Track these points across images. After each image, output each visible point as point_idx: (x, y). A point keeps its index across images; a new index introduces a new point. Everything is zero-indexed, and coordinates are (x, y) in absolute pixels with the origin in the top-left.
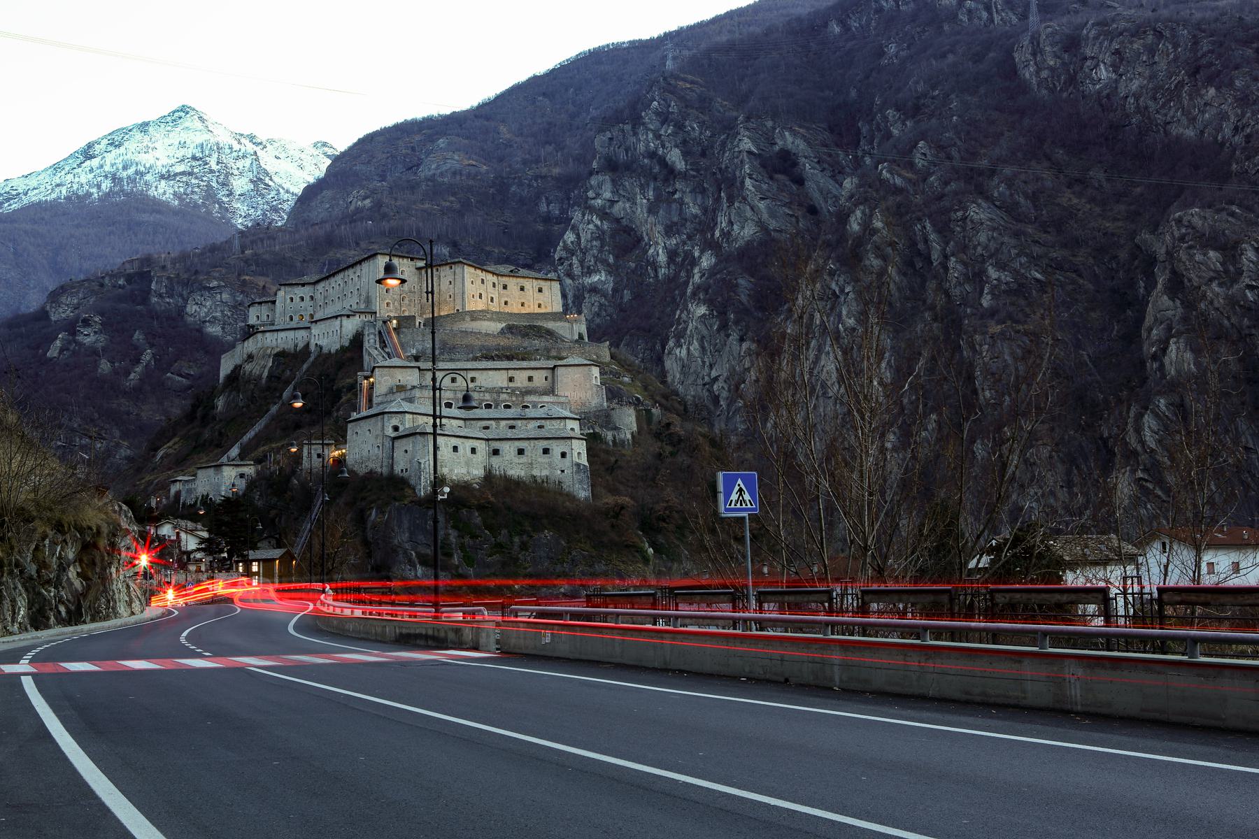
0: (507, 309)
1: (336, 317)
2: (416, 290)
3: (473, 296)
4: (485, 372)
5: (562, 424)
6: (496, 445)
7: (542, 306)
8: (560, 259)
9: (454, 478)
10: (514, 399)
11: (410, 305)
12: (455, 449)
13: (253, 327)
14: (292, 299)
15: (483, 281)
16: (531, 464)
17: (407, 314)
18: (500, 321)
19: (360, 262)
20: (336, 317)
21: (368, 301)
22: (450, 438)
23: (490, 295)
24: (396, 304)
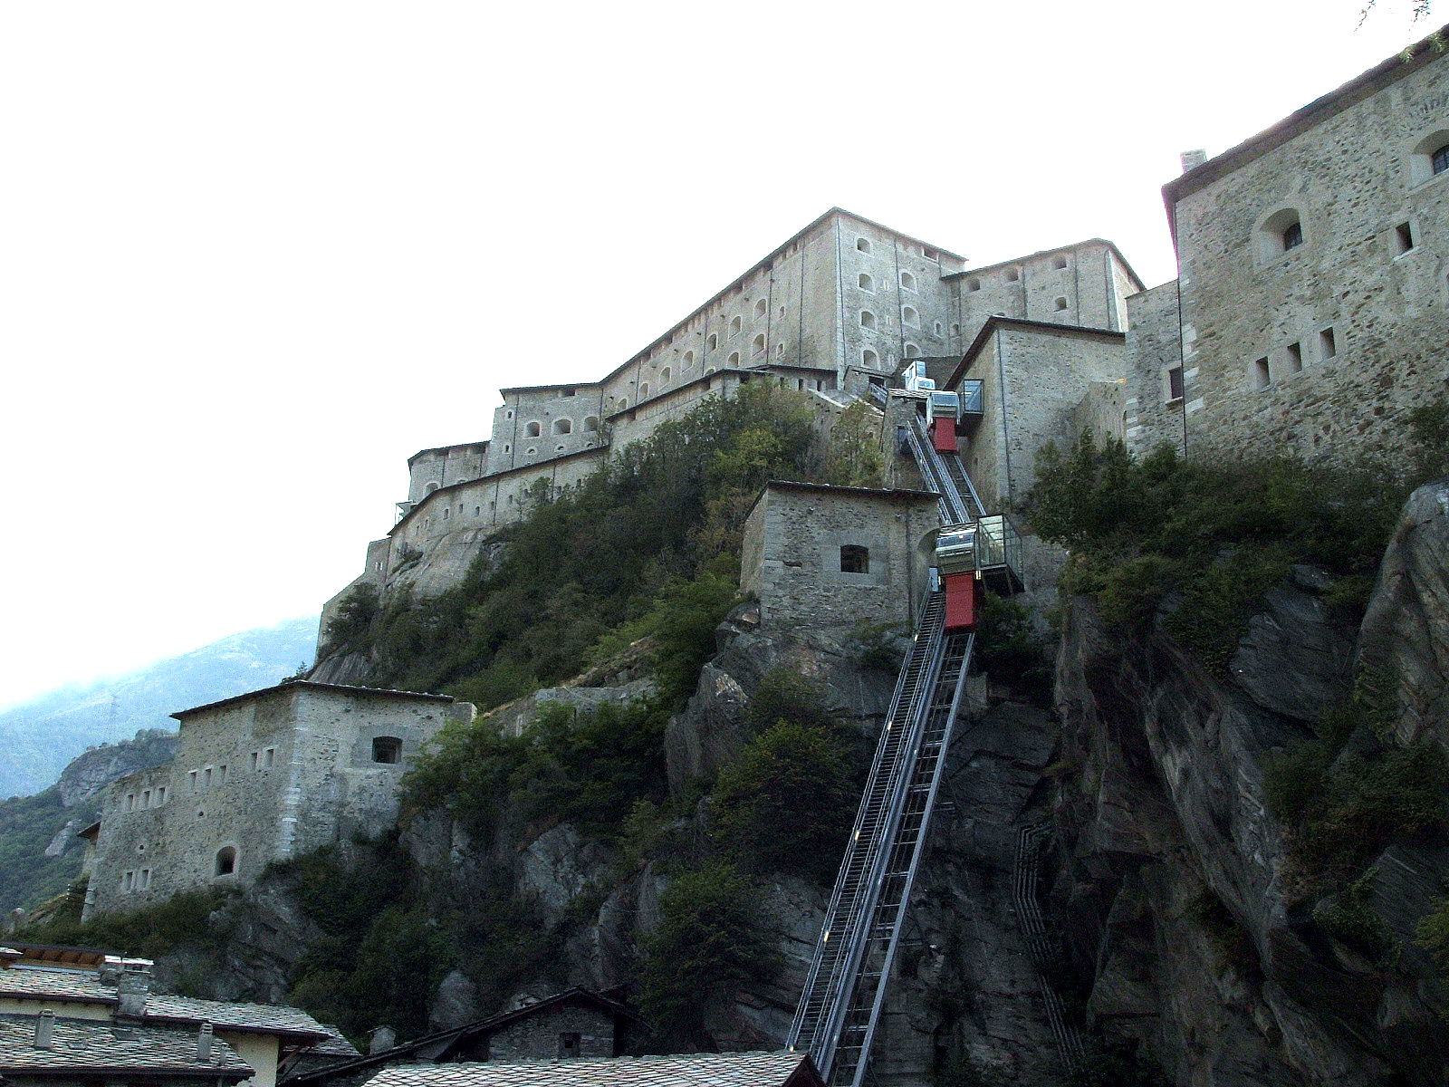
14: (534, 431)
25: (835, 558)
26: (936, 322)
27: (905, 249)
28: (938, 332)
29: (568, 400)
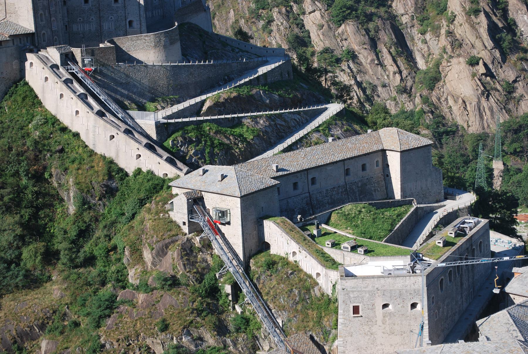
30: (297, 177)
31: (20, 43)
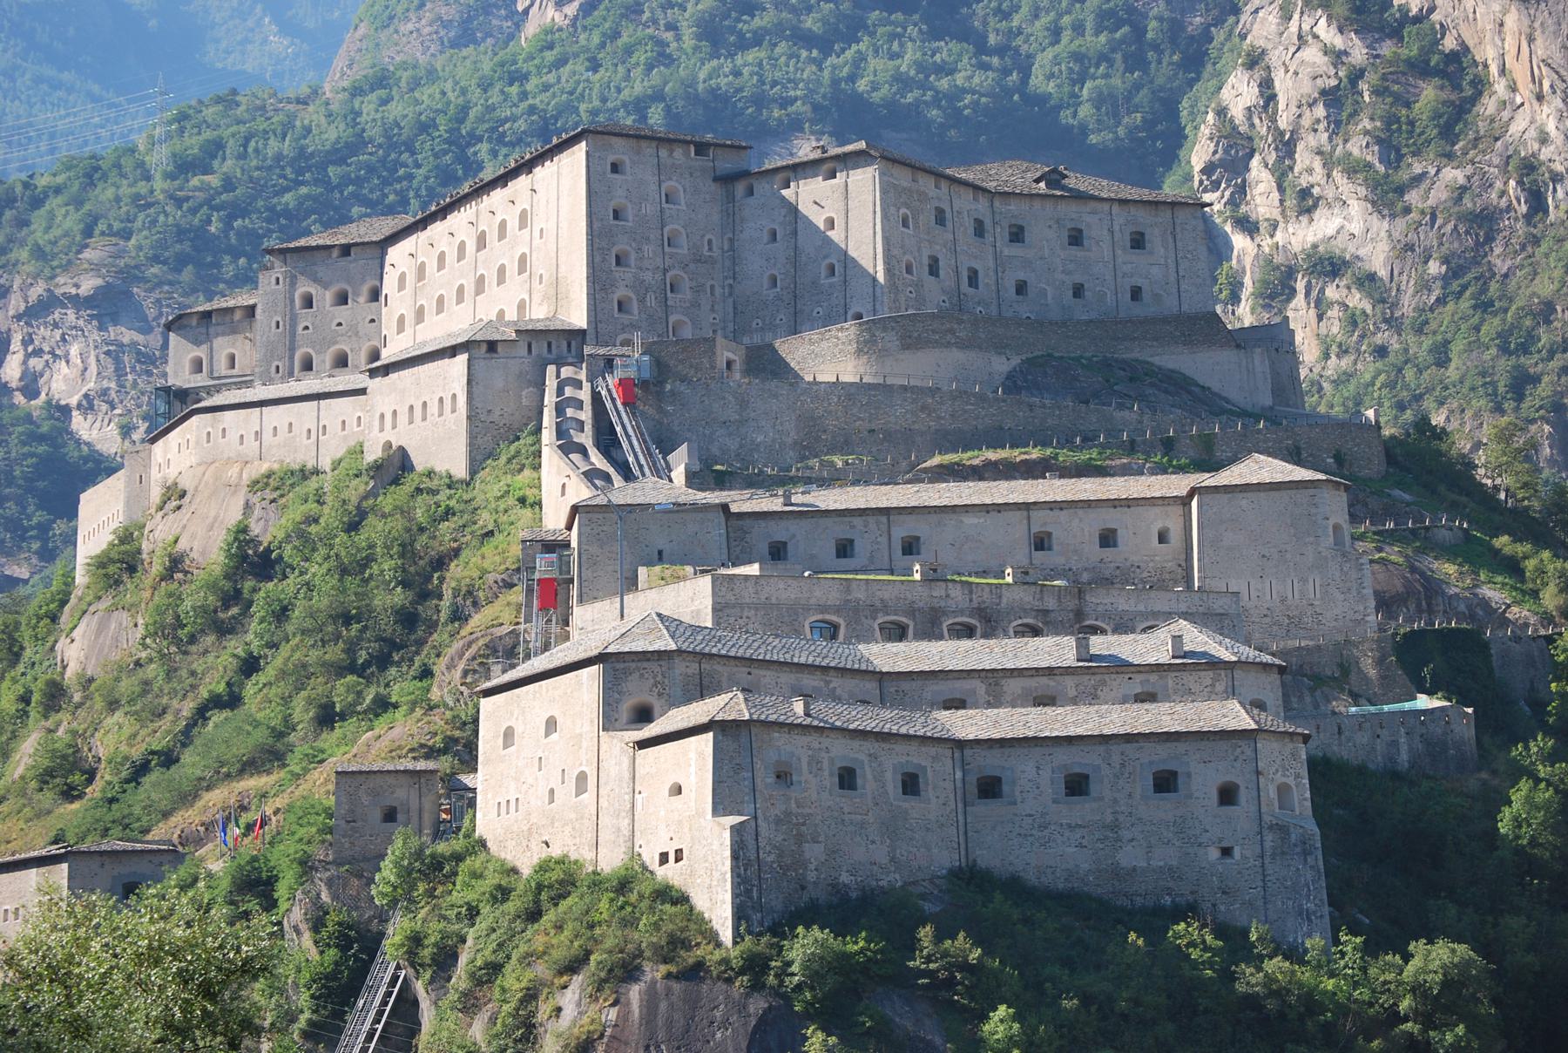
0: (1024, 309)
1: (452, 351)
2: (716, 253)
3: (909, 270)
4: (950, 520)
5: (1220, 687)
6: (991, 763)
7: (1146, 296)
8: (1208, 170)
9: (845, 878)
10: (1051, 603)
11: (696, 304)
12: (847, 779)
13: (183, 395)
14: (308, 302)
15: (940, 217)
16: (1115, 827)
17: (687, 333)
18: (1000, 348)
19: (527, 167)
20: (452, 351)
21: (557, 293)
22: (826, 742)
23: (965, 263)
24: (651, 300)
25: (377, 814)
26: (708, 237)
27: (671, 155)
28: (710, 249)
29: (344, 262)
30: (853, 527)
31: (550, 350)
